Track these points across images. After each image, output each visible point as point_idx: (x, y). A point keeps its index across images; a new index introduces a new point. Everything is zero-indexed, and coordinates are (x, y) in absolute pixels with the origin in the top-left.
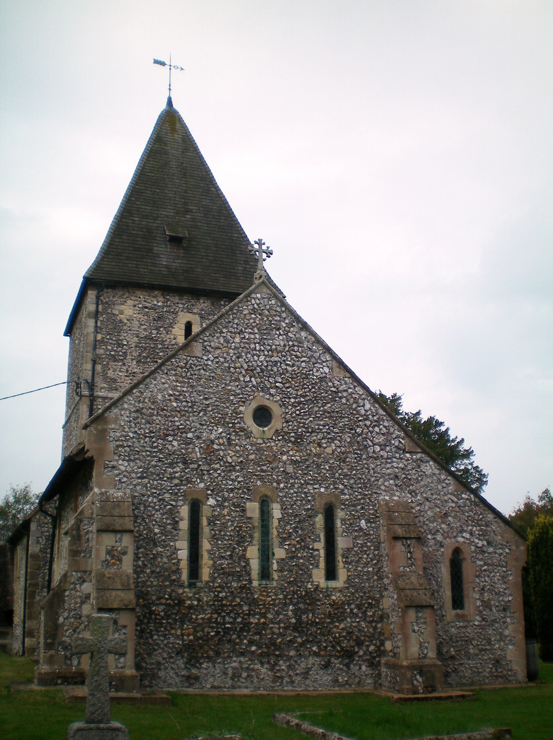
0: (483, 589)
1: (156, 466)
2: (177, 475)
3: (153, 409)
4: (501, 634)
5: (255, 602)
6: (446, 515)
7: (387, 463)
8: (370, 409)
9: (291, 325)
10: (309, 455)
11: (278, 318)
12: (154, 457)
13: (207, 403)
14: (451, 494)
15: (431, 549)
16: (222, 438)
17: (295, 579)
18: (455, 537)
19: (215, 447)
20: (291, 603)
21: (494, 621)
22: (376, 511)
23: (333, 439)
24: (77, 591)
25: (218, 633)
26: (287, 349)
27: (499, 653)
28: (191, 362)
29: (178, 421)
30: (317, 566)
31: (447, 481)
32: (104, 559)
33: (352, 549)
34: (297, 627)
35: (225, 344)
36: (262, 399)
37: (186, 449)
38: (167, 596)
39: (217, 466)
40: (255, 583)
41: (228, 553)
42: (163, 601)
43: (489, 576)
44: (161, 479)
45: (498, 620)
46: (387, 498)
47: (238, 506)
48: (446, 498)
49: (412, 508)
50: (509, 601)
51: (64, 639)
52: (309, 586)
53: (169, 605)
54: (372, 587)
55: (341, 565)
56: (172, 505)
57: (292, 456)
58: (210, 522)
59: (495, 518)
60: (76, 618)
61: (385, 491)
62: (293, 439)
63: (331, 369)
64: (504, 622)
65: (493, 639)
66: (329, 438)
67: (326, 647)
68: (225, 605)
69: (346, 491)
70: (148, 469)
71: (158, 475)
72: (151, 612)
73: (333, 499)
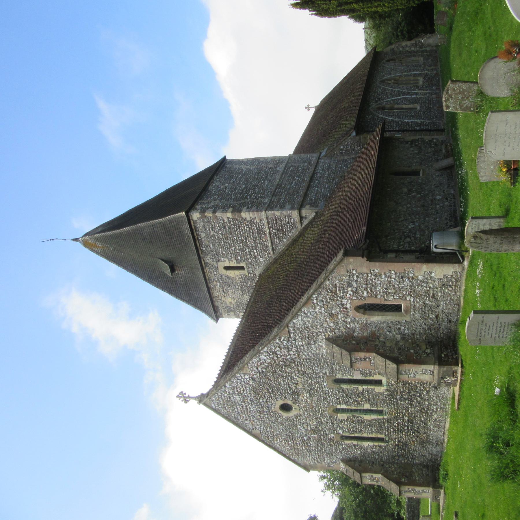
0: (386, 293)
4: (422, 282)
5: (396, 418)
6: (332, 315)
7: (300, 348)
15: (358, 326)
18: (346, 308)
19: (309, 429)
23: (291, 377)
27: (437, 284)
30: (374, 389)
31: (306, 312)
33: (361, 371)
34: (411, 400)
40: (385, 417)
43: (376, 288)
45: (411, 283)
50: (396, 274)
55: (372, 378)
59: (329, 280)
61: (320, 350)
63: (245, 374)
65: (425, 289)
67: (424, 387)
68: (398, 429)
69: (324, 372)
72: (402, 455)
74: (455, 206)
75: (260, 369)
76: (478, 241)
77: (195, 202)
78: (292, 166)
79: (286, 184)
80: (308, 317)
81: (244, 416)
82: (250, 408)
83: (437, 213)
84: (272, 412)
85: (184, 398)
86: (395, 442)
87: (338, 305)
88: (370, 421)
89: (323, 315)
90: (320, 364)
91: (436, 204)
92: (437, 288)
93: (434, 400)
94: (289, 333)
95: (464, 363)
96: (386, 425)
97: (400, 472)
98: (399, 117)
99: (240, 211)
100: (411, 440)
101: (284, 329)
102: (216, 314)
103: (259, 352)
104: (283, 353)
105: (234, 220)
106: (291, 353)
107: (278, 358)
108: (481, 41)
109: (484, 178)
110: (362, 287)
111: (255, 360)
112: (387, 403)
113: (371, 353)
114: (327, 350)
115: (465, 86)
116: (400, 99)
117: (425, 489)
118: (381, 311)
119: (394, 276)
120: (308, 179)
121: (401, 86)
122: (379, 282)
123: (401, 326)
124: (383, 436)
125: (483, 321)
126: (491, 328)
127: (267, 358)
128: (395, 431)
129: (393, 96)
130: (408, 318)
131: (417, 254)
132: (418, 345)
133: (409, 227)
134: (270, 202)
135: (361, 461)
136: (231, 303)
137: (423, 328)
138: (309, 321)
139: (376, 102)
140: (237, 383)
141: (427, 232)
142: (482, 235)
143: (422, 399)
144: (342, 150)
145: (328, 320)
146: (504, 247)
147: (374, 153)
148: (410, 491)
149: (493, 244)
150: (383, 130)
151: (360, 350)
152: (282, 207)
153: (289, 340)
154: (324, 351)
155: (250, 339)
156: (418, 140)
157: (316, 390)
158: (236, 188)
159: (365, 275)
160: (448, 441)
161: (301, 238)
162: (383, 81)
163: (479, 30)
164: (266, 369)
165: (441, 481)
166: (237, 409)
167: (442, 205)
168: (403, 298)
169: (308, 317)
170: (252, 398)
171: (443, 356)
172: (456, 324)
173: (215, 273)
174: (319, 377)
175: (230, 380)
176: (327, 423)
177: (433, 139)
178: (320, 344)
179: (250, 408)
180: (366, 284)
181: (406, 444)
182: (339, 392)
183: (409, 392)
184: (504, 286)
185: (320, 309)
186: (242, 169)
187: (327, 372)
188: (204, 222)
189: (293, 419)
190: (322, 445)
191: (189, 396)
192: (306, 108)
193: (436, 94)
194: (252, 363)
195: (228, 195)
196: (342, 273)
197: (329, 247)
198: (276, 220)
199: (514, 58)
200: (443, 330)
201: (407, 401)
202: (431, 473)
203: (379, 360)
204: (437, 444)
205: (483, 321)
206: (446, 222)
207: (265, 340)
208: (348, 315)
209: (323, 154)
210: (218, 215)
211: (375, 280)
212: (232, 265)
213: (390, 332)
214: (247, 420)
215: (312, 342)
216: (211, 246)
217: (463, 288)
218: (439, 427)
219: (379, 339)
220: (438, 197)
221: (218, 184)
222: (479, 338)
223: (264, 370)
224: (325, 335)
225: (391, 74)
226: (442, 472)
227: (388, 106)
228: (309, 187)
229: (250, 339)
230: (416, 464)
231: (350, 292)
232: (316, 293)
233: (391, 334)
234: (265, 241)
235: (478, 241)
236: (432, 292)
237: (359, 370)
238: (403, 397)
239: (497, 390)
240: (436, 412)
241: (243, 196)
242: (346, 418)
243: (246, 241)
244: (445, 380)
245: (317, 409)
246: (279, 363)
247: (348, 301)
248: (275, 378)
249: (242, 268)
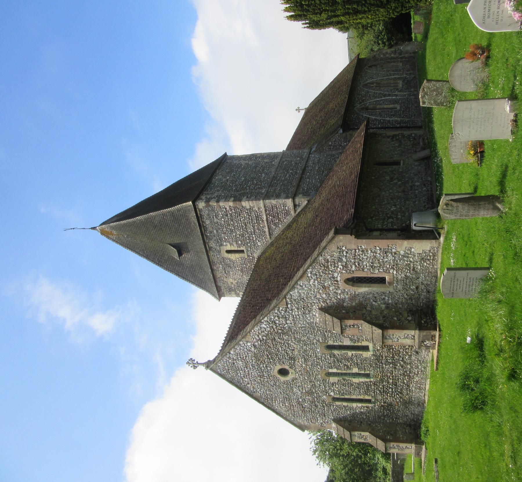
0: (372, 267)
5: (382, 380)
6: (324, 287)
7: (296, 318)
18: (337, 281)
19: (304, 391)
21: (394, 260)
23: (288, 344)
25: (397, 394)
27: (417, 258)
29: (294, 403)
30: (362, 354)
31: (301, 284)
33: (350, 338)
34: (395, 364)
40: (372, 380)
43: (363, 262)
49: (322, 306)
50: (380, 249)
55: (360, 344)
57: (302, 362)
59: (322, 256)
63: (247, 342)
67: (406, 352)
72: (387, 415)
74: (432, 191)
75: (260, 337)
76: (450, 208)
77: (201, 193)
78: (286, 161)
79: (281, 176)
80: (303, 289)
81: (246, 380)
82: (252, 373)
83: (416, 197)
84: (271, 376)
85: (193, 364)
86: (380, 403)
87: (330, 278)
88: (359, 384)
89: (317, 287)
90: (314, 332)
91: (415, 190)
92: (417, 262)
93: (415, 364)
94: (287, 304)
95: (441, 327)
96: (373, 387)
97: (385, 431)
98: (381, 116)
99: (240, 200)
100: (395, 400)
101: (282, 300)
102: (219, 293)
103: (260, 321)
104: (281, 322)
105: (235, 208)
106: (288, 322)
107: (277, 326)
108: (452, 46)
109: (455, 160)
110: (351, 261)
111: (256, 329)
112: (373, 367)
113: (359, 321)
114: (320, 319)
115: (438, 84)
116: (382, 100)
117: (409, 445)
118: (368, 283)
120: (301, 172)
121: (382, 89)
122: (366, 257)
123: (385, 296)
124: (370, 398)
125: (455, 276)
126: (462, 282)
127: (267, 327)
128: (381, 392)
129: (376, 97)
130: (391, 289)
131: (399, 232)
132: (400, 313)
133: (392, 209)
134: (267, 192)
135: (351, 421)
136: (232, 283)
137: (405, 298)
138: (304, 293)
139: (361, 103)
140: (241, 349)
141: (407, 214)
142: (452, 202)
143: (405, 362)
144: (330, 146)
145: (321, 291)
146: (471, 213)
147: (360, 146)
148: (394, 448)
149: (462, 211)
150: (367, 125)
151: (349, 318)
152: (278, 197)
153: (286, 310)
154: (318, 320)
155: (251, 312)
156: (398, 135)
157: (311, 356)
158: (237, 181)
159: (353, 251)
160: (429, 400)
161: (295, 224)
162: (366, 85)
163: (450, 37)
164: (266, 337)
165: (423, 438)
166: (240, 373)
167: (420, 190)
168: (387, 271)
169: (303, 289)
171: (423, 322)
172: (434, 293)
173: (218, 256)
174: (313, 344)
175: (234, 347)
176: (320, 385)
177: (412, 134)
178: (314, 313)
179: (252, 373)
180: (355, 259)
181: (390, 405)
182: (330, 357)
183: (393, 357)
184: (473, 252)
185: (314, 282)
186: (241, 164)
187: (320, 339)
188: (209, 210)
190: (316, 406)
191: (197, 362)
192: (296, 110)
193: (414, 95)
194: (254, 331)
195: (230, 186)
197: (321, 229)
198: (272, 208)
199: (479, 59)
200: (423, 300)
201: (391, 365)
202: (412, 430)
203: (366, 327)
204: (419, 405)
205: (455, 276)
206: (423, 205)
207: (265, 311)
208: (338, 287)
209: (314, 149)
210: (221, 204)
211: (362, 255)
212: (233, 248)
213: (376, 302)
214: (248, 383)
215: (307, 312)
216: (215, 231)
217: (440, 261)
218: (420, 389)
219: (365, 308)
220: (417, 184)
221: (221, 177)
222: (452, 291)
223: (265, 338)
224: (318, 306)
225: (373, 78)
226: (423, 429)
227: (371, 107)
228: (301, 179)
229: (251, 312)
230: (400, 423)
231: (340, 266)
232: (311, 267)
233: (376, 304)
234: (263, 227)
235: (450, 208)
237: (349, 337)
238: (387, 361)
239: (469, 339)
240: (417, 375)
241: (243, 187)
242: (337, 381)
243: (246, 227)
244: (425, 343)
245: (311, 373)
246: (278, 331)
247: (338, 274)
248: (274, 345)
249: (242, 251)
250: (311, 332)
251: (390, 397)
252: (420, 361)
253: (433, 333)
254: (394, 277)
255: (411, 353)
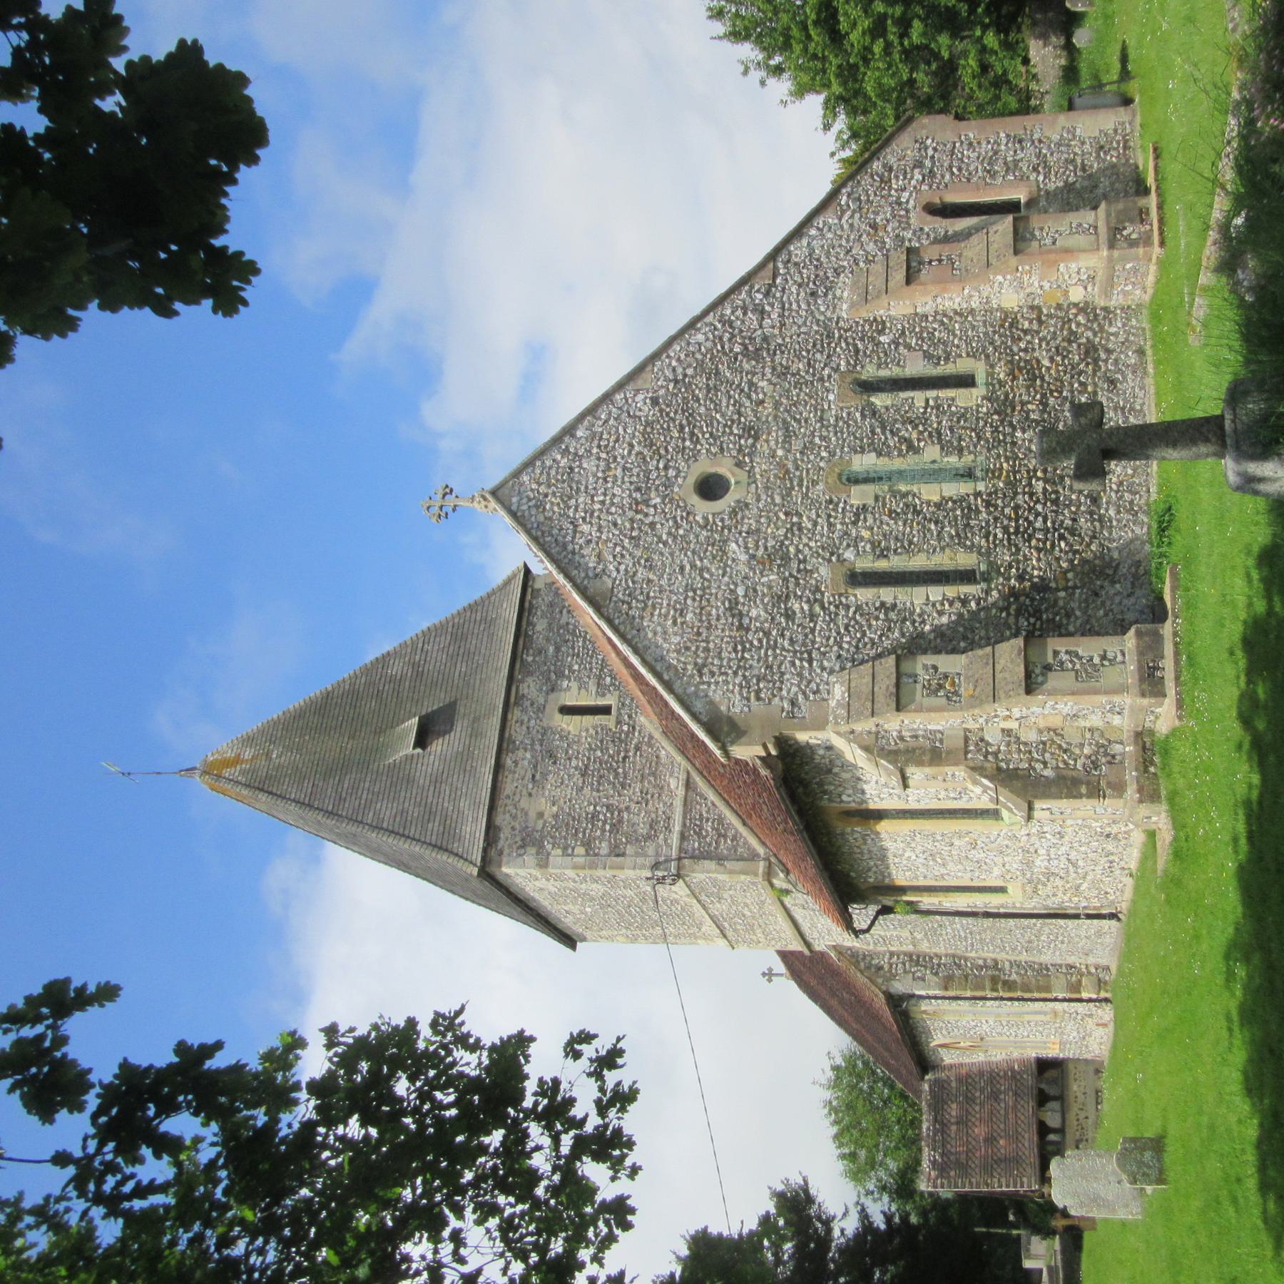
0: (989, 172)
1: (791, 639)
2: (806, 607)
3: (697, 648)
4: (1059, 145)
6: (874, 226)
7: (790, 309)
8: (705, 334)
9: (566, 452)
10: (776, 417)
11: (553, 472)
12: (776, 642)
13: (688, 567)
14: (840, 219)
16: (746, 543)
17: (973, 430)
18: (907, 211)
19: (761, 552)
20: (1013, 436)
22: (865, 321)
23: (751, 384)
24: (999, 751)
25: (1062, 537)
26: (604, 455)
28: (620, 595)
29: (717, 608)
30: (953, 399)
32: (944, 699)
35: (593, 545)
36: (685, 488)
37: (764, 595)
38: (1004, 615)
39: (792, 549)
40: (981, 487)
41: (933, 527)
42: (1012, 620)
43: (968, 165)
44: (813, 631)
46: (845, 307)
47: (857, 515)
48: (846, 227)
50: (1008, 136)
51: (1079, 767)
52: (985, 410)
53: (1018, 613)
54: (985, 322)
56: (855, 613)
57: (777, 442)
58: (883, 555)
60: (1044, 751)
62: (750, 441)
63: (637, 391)
64: (1040, 141)
66: (750, 389)
67: (1081, 384)
68: (1017, 528)
70: (795, 652)
71: (806, 636)
73: (849, 380)
90: (829, 344)
107: (733, 336)
119: (1004, 141)
170: (633, 457)
174: (821, 379)
176: (815, 524)
181: (1042, 586)
182: (863, 416)
189: (722, 520)
196: (905, 144)
208: (908, 223)
236: (1079, 161)
238: (1027, 418)
250: (822, 346)
251: (1039, 550)
252: (1123, 409)
253: (1142, 202)
254: (1039, 189)
255: (1095, 385)
